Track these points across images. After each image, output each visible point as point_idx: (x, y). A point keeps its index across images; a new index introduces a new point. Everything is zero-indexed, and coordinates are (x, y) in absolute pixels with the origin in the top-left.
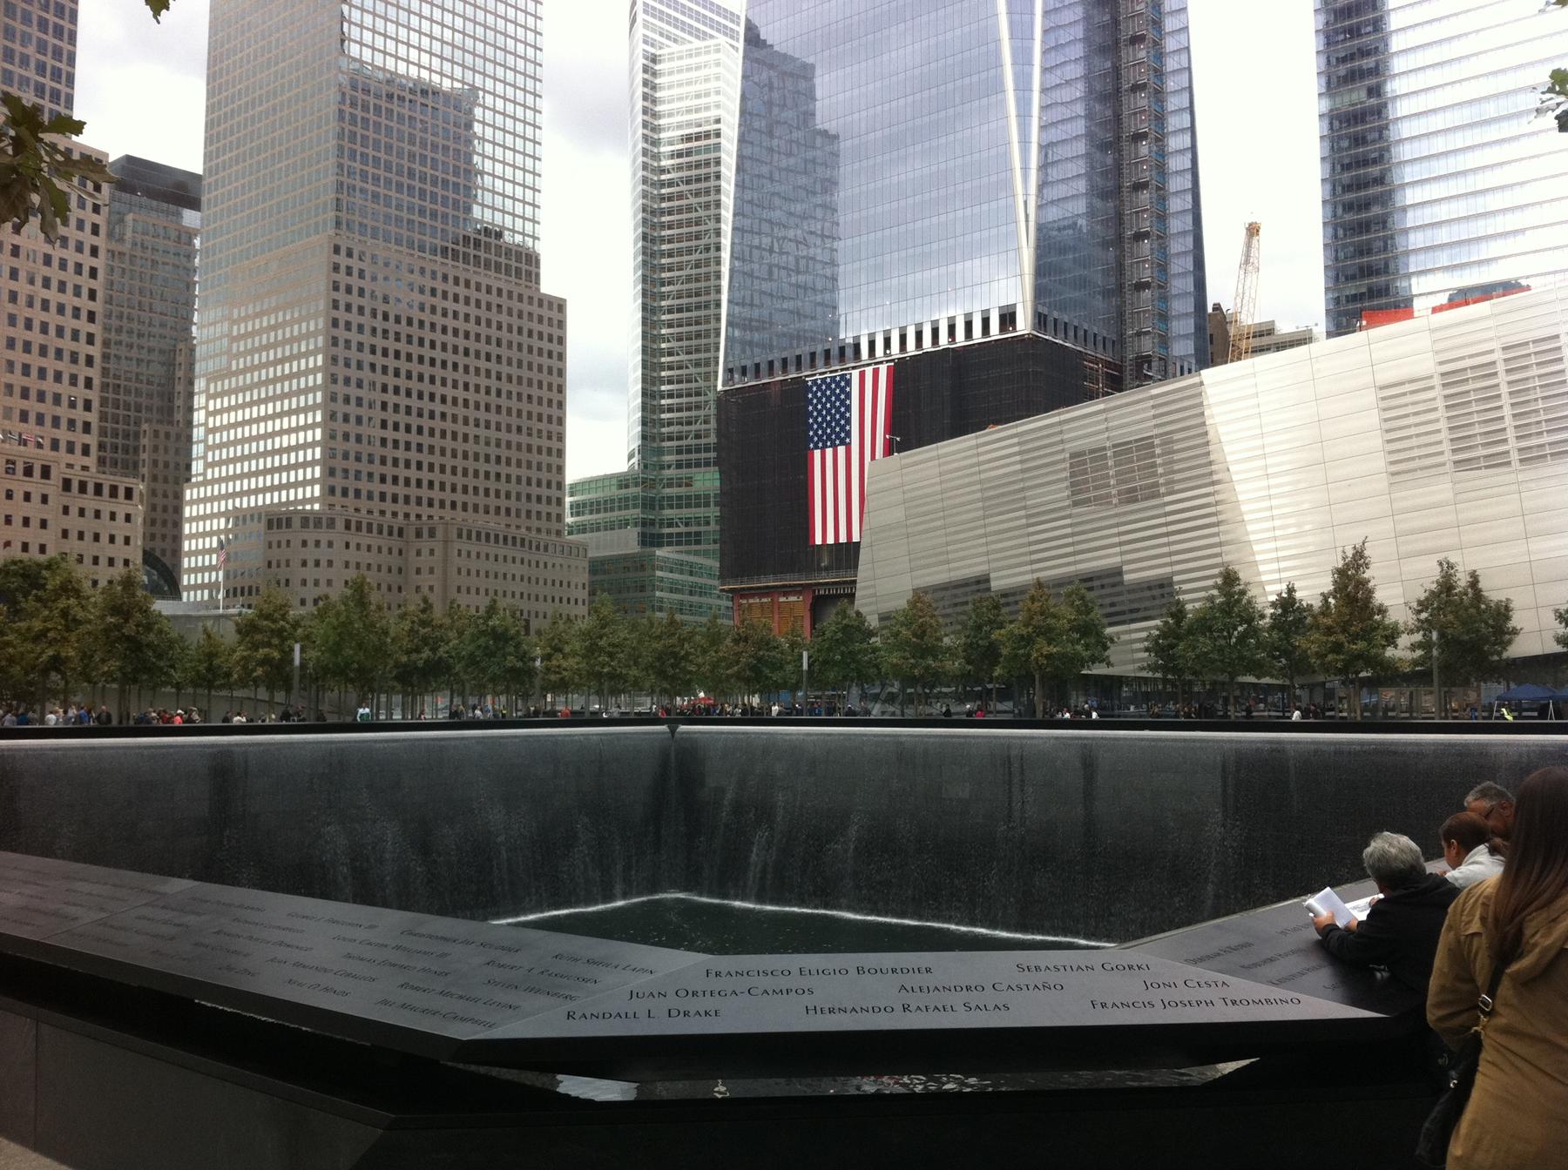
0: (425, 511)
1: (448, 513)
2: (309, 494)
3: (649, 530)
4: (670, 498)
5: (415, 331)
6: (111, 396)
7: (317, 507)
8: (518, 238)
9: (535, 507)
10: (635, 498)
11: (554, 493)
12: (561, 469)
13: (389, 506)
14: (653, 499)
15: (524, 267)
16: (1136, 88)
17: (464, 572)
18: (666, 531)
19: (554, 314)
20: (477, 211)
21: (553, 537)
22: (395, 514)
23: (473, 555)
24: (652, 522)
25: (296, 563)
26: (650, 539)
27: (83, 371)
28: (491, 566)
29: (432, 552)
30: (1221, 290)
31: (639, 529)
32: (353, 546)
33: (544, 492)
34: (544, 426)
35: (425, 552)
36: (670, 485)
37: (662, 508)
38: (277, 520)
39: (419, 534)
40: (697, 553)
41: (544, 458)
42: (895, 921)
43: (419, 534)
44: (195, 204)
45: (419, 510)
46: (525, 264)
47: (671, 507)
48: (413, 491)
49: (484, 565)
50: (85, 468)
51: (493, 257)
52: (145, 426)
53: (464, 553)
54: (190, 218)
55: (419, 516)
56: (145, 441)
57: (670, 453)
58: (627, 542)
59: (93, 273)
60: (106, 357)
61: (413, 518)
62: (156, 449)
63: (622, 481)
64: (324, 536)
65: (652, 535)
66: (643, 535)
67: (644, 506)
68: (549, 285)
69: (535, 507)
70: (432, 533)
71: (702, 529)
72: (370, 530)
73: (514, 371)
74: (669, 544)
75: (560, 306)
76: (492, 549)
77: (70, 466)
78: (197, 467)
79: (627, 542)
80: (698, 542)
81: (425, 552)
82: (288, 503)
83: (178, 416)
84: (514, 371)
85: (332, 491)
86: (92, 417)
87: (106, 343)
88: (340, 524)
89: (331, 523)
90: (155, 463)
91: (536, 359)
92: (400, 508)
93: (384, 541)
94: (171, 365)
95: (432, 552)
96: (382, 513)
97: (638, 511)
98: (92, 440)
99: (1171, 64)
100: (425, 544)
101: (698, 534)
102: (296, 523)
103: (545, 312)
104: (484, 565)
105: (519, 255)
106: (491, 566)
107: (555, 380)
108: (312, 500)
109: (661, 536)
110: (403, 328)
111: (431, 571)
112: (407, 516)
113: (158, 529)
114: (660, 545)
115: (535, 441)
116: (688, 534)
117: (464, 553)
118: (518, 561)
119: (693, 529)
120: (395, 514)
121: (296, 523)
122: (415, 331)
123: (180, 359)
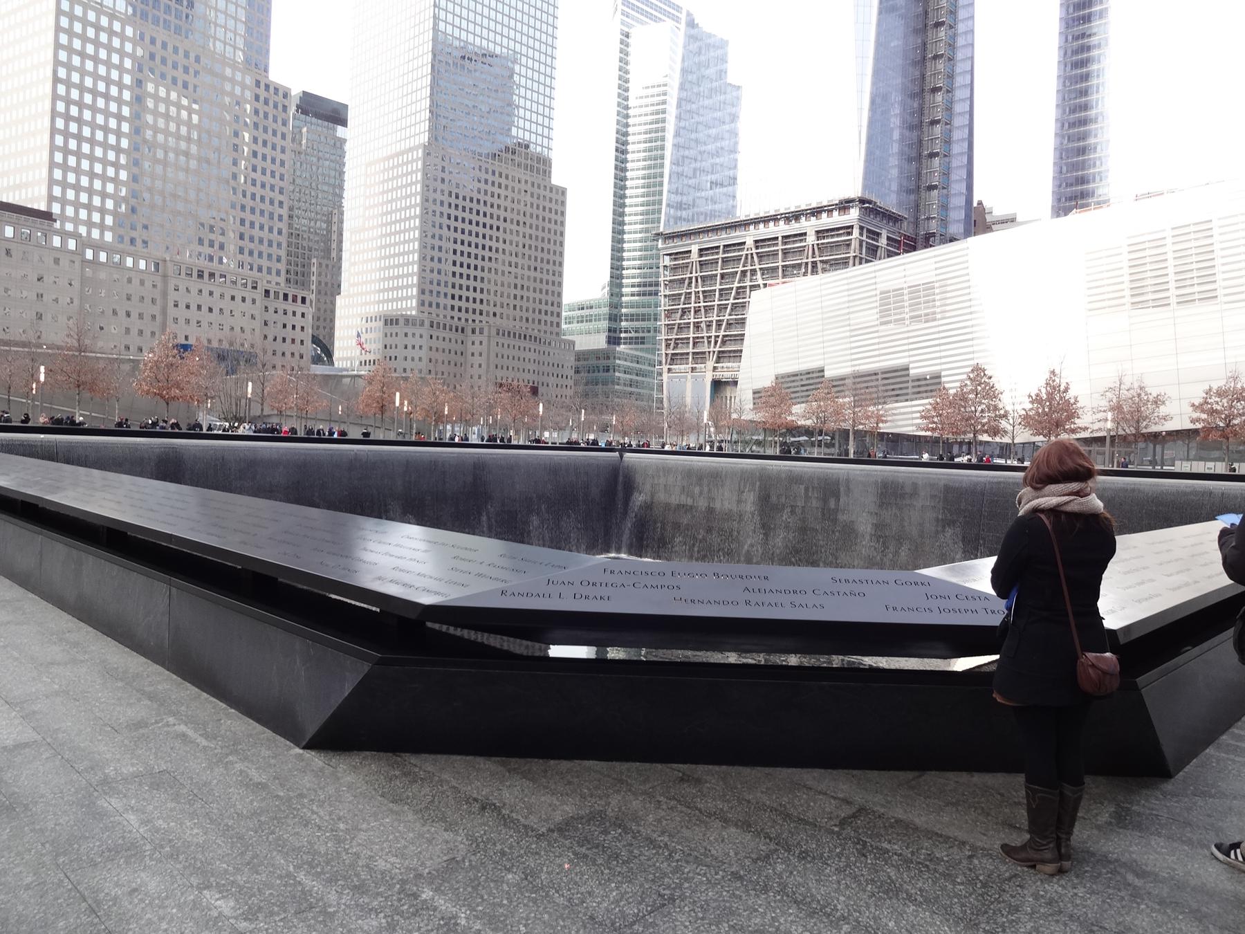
1: (491, 319)
2: (410, 306)
3: (612, 335)
5: (475, 206)
6: (294, 240)
7: (414, 313)
8: (539, 149)
9: (543, 317)
11: (555, 309)
12: (560, 295)
13: (456, 314)
15: (541, 167)
16: (936, 57)
18: (623, 335)
19: (560, 198)
20: (514, 131)
21: (554, 336)
22: (459, 319)
25: (401, 347)
26: (613, 340)
27: (278, 225)
28: (516, 353)
30: (980, 194)
33: (549, 308)
34: (550, 267)
35: (477, 343)
38: (390, 321)
39: (473, 332)
40: (641, 350)
41: (550, 287)
43: (473, 332)
44: (343, 122)
45: (474, 317)
46: (542, 165)
48: (471, 305)
49: (512, 352)
51: (523, 161)
52: (314, 260)
54: (340, 131)
56: (314, 269)
58: (599, 342)
59: (282, 163)
60: (290, 217)
62: (320, 274)
64: (418, 331)
66: (609, 337)
67: (610, 319)
68: (557, 179)
69: (543, 317)
71: (646, 335)
72: (445, 328)
73: (533, 232)
75: (563, 192)
76: (517, 343)
77: (269, 282)
79: (599, 342)
80: (643, 343)
81: (477, 343)
82: (397, 309)
83: (334, 254)
84: (533, 232)
85: (423, 304)
86: (283, 253)
87: (291, 209)
88: (427, 323)
89: (422, 324)
90: (320, 283)
91: (547, 225)
92: (463, 315)
93: (453, 335)
94: (329, 223)
96: (452, 318)
98: (282, 267)
99: (960, 41)
100: (477, 338)
101: (643, 338)
102: (401, 322)
103: (554, 196)
104: (512, 352)
105: (539, 160)
106: (516, 353)
107: (558, 238)
108: (411, 309)
110: (468, 204)
111: (481, 354)
112: (467, 320)
113: (321, 323)
115: (545, 277)
116: (637, 338)
119: (641, 335)
120: (459, 319)
121: (401, 322)
122: (475, 206)
123: (335, 219)
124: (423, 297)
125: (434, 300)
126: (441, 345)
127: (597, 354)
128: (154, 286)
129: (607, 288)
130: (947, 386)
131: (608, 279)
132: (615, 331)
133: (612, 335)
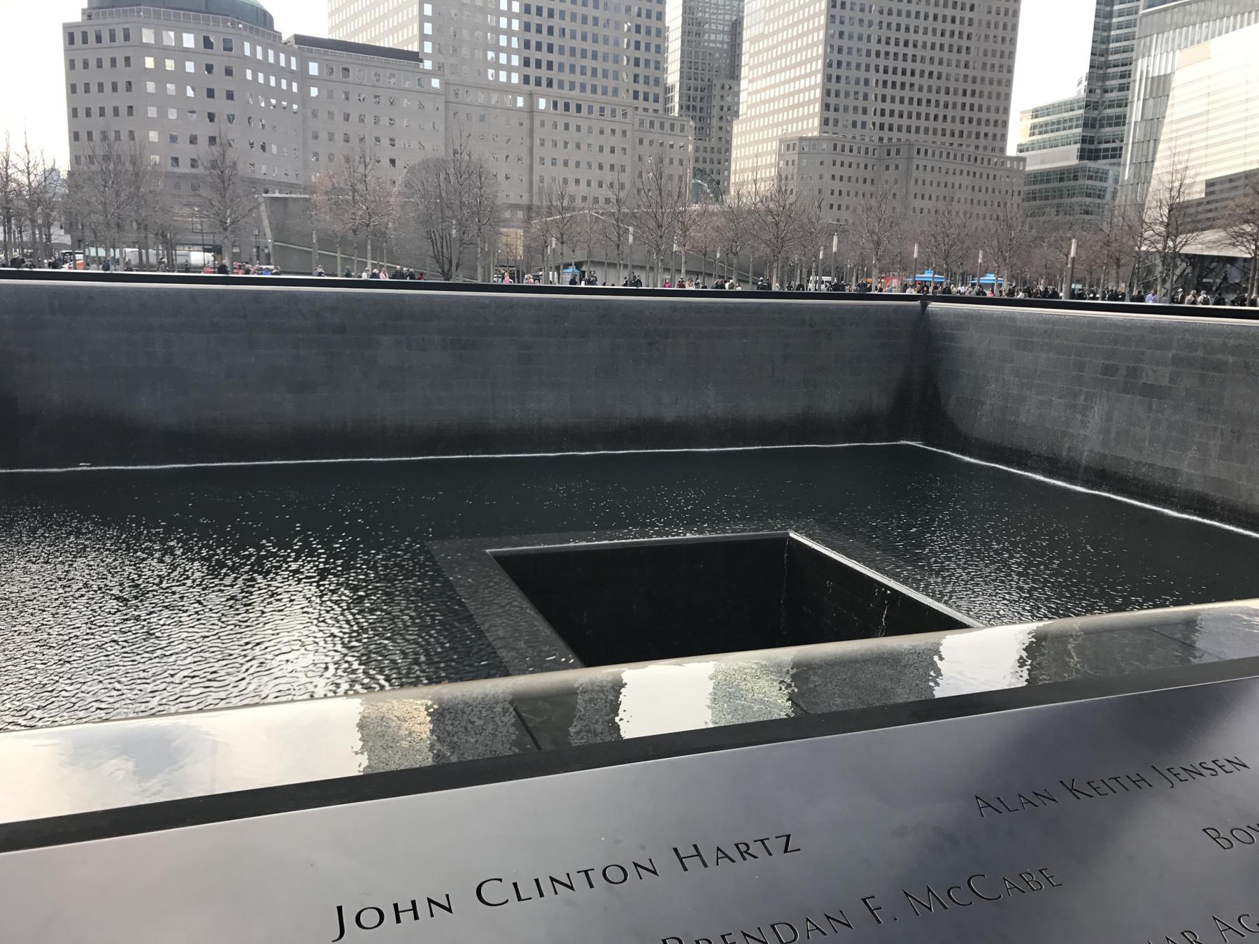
0: (895, 135)
3: (1087, 146)
4: (1110, 118)
10: (1078, 119)
14: (1094, 119)
17: (920, 182)
21: (989, 152)
23: (929, 168)
24: (1091, 141)
29: (897, 167)
31: (1078, 146)
32: (838, 163)
36: (1110, 106)
37: (1102, 126)
42: (1200, 520)
47: (1110, 125)
50: (656, 111)
53: (921, 167)
55: (890, 139)
57: (1114, 78)
58: (1068, 157)
61: (885, 141)
63: (1069, 106)
65: (1090, 151)
66: (1082, 150)
67: (1085, 125)
70: (898, 152)
74: (1105, 157)
78: (743, 108)
79: (1068, 157)
95: (897, 167)
97: (1080, 130)
109: (1098, 150)
114: (1097, 158)
117: (921, 167)
118: (965, 173)
124: (827, 114)
125: (544, 73)
126: (846, 172)
127: (1063, 175)
128: (521, 124)
129: (1085, 83)
130: (1205, 24)
131: (1087, 70)
132: (1091, 142)
133: (1087, 146)
